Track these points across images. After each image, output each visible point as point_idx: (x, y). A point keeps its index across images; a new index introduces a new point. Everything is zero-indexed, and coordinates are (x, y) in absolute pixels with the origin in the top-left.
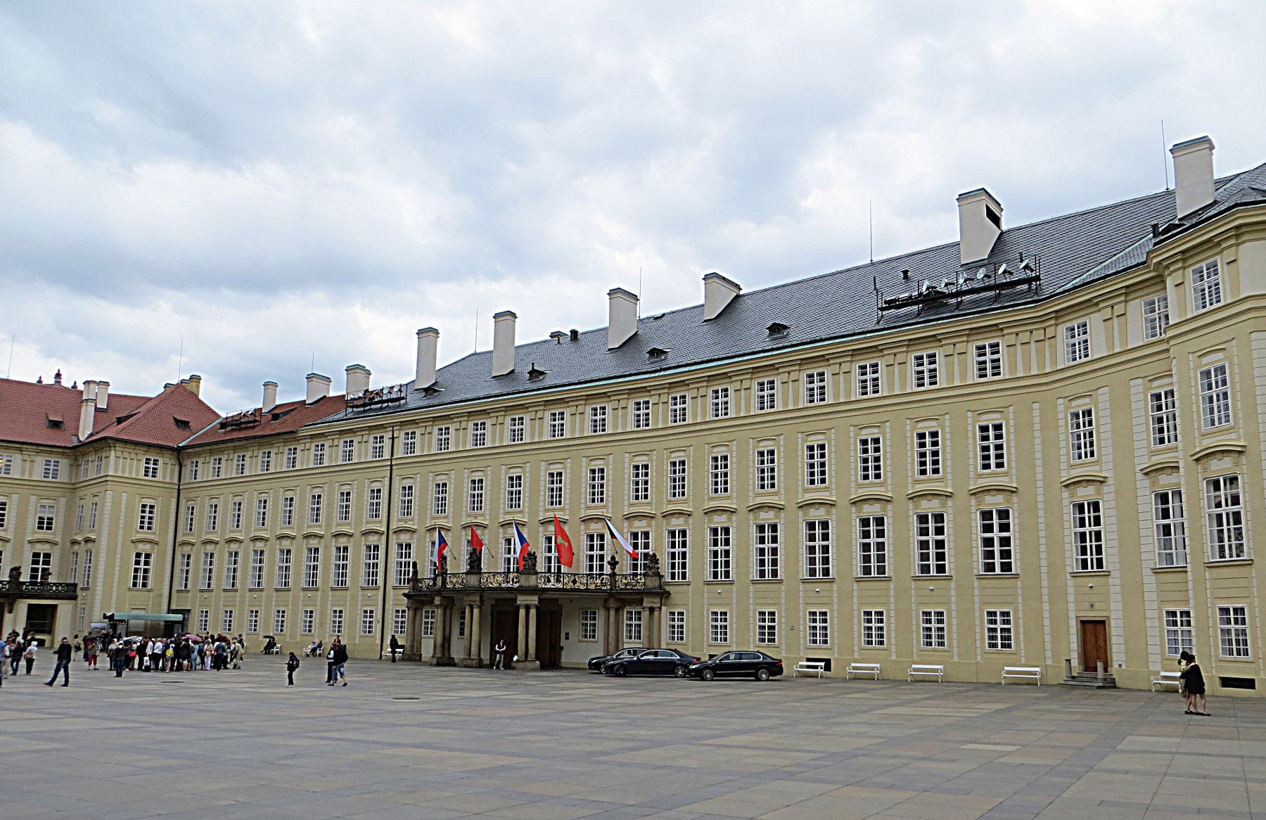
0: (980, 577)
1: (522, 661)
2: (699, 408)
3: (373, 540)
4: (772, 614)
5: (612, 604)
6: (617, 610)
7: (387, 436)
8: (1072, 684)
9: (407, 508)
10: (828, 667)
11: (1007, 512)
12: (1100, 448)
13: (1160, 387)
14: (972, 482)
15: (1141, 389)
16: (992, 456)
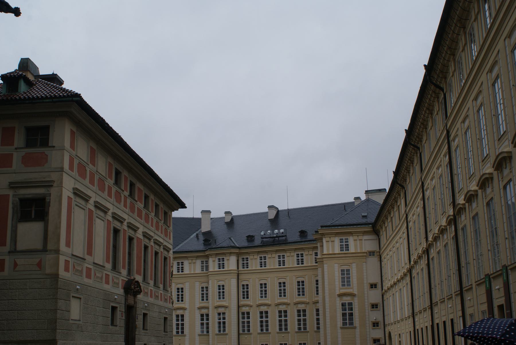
13: (204, 285)
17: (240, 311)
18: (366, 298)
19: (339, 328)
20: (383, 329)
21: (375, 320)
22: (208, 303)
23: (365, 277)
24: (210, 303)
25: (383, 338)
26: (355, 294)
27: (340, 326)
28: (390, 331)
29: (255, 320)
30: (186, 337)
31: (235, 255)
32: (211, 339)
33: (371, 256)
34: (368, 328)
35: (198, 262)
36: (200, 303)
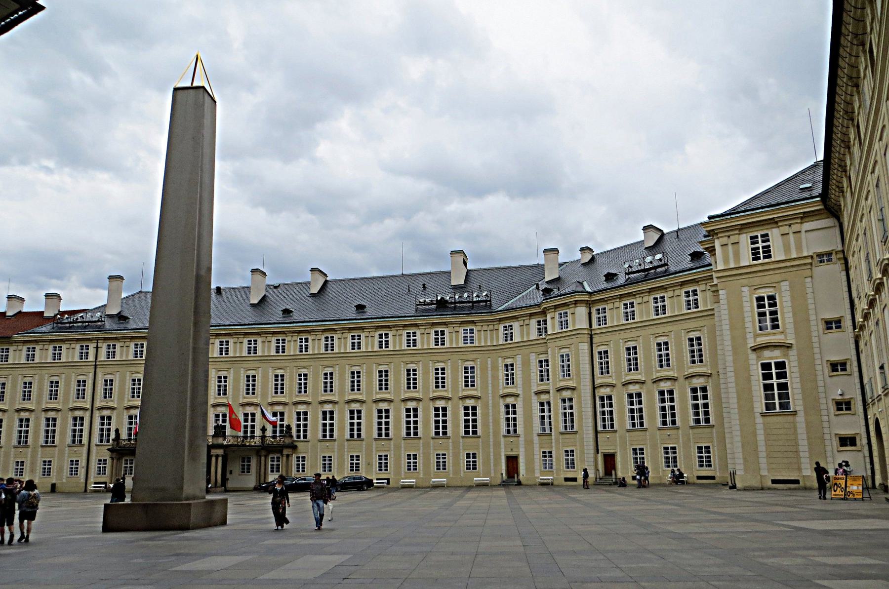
0: (463, 437)
1: (214, 488)
2: (316, 346)
3: (78, 414)
4: (387, 456)
5: (263, 453)
6: (266, 457)
7: (92, 346)
8: (504, 484)
9: (108, 394)
10: (388, 483)
11: (476, 407)
12: (516, 381)
13: (543, 358)
14: (460, 393)
15: (534, 357)
16: (469, 382)
17: (596, 395)
18: (816, 350)
19: (758, 415)
20: (862, 416)
21: (840, 395)
22: (549, 384)
23: (812, 307)
24: (551, 384)
25: (864, 435)
26: (791, 344)
27: (760, 411)
28: (878, 416)
29: (621, 408)
30: (520, 439)
31: (584, 305)
32: (553, 441)
33: (824, 262)
34: (824, 413)
35: (533, 322)
36: (538, 385)
